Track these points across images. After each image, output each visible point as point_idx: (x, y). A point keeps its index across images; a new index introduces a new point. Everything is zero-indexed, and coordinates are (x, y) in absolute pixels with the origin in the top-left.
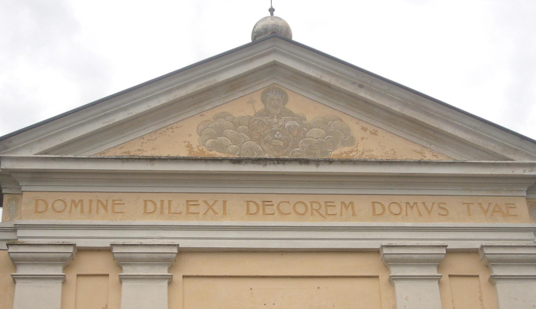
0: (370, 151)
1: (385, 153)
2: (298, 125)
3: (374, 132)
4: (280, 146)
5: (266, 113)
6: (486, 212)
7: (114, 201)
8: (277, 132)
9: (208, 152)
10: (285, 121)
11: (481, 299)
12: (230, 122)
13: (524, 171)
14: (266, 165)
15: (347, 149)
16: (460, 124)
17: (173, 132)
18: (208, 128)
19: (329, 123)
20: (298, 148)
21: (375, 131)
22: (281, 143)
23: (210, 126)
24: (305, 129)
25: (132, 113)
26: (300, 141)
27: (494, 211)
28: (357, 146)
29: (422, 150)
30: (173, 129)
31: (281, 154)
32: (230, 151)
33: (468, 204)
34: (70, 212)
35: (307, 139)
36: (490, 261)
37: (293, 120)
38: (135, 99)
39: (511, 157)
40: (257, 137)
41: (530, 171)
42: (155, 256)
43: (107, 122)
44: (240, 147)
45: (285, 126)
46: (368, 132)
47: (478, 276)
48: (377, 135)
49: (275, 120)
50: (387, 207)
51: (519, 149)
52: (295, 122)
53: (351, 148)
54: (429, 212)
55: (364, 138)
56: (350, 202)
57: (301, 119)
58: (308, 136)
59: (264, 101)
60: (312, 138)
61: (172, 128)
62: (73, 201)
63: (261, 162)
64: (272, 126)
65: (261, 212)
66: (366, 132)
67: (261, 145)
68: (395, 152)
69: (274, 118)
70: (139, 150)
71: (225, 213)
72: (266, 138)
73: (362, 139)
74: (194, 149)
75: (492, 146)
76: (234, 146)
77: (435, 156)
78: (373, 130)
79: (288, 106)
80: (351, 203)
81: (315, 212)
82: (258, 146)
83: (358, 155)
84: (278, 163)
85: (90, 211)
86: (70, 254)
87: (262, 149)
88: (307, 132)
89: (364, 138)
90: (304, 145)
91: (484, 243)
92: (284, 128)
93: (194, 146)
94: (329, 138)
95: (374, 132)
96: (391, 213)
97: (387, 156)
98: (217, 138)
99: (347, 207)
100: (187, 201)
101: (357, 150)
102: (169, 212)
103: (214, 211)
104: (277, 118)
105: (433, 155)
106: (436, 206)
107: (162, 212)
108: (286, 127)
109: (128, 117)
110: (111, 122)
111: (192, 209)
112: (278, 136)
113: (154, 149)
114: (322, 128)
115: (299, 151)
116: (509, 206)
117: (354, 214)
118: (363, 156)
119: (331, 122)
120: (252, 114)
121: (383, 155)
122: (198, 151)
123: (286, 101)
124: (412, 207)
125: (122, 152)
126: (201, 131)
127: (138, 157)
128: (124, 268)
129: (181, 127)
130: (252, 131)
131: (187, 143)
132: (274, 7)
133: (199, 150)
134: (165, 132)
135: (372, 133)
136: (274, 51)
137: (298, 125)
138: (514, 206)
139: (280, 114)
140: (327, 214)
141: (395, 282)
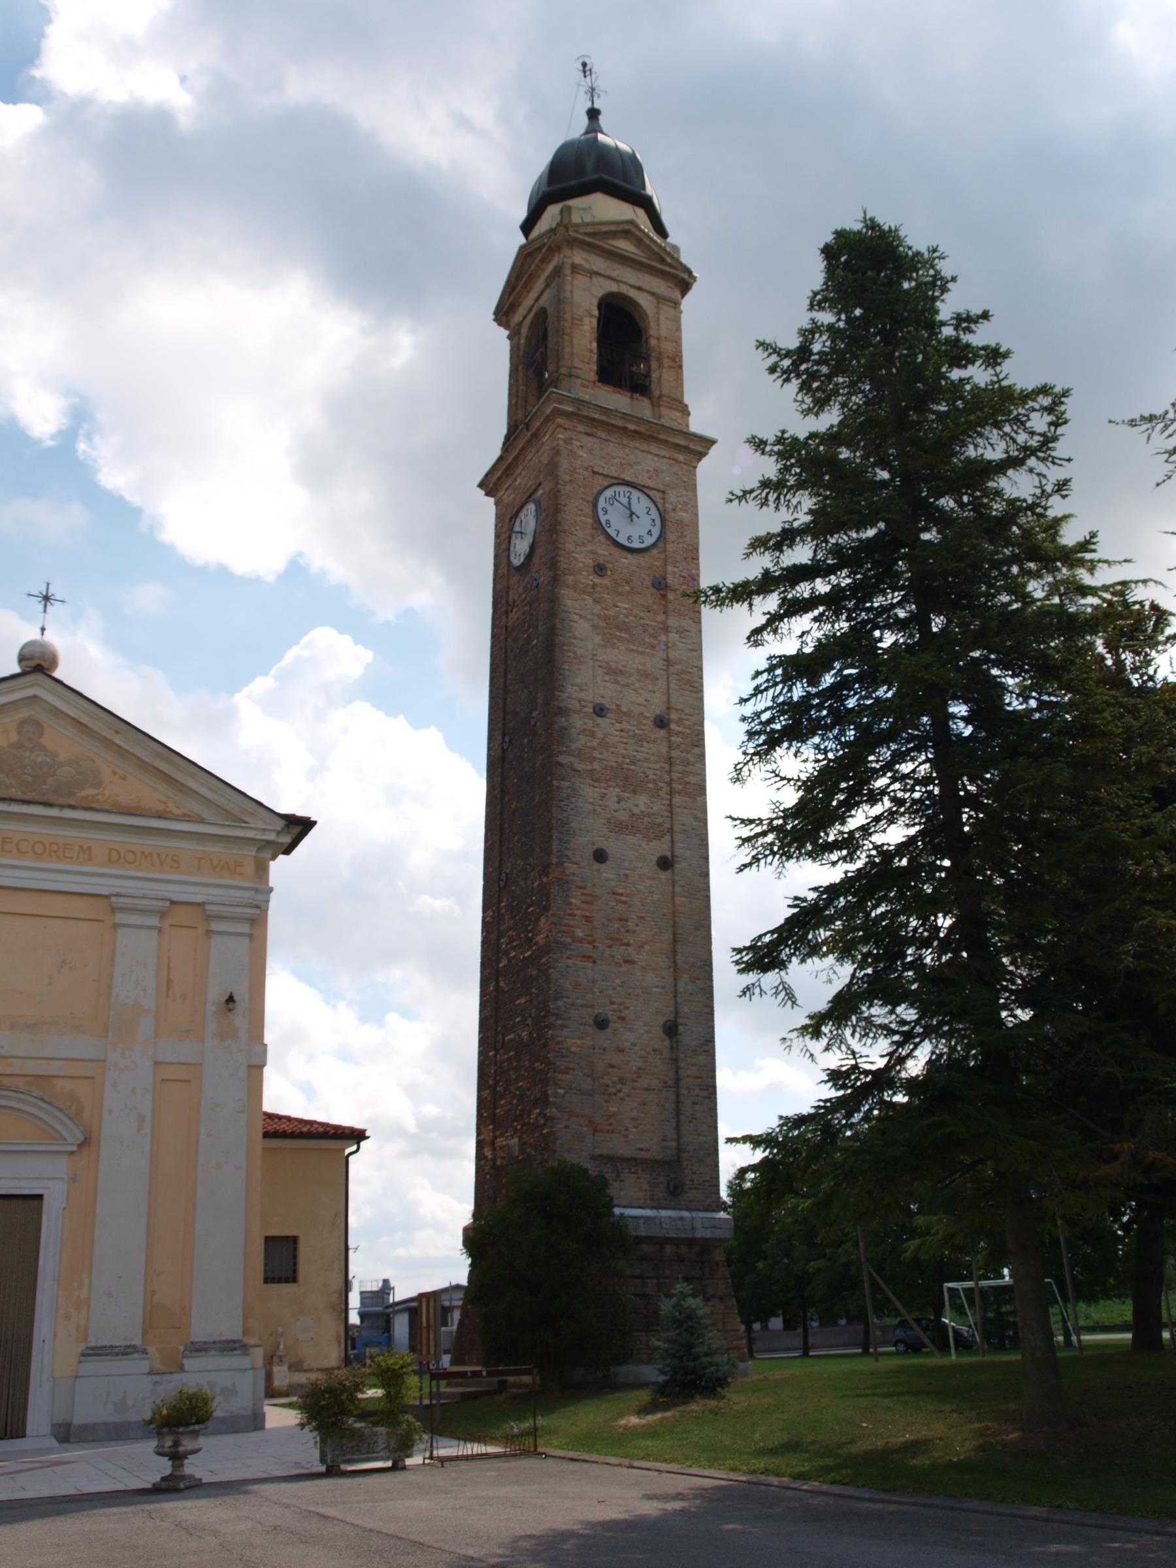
6: (214, 868)
15: (93, 791)
22: (30, 779)
33: (200, 858)
39: (246, 819)
47: (196, 928)
49: (28, 754)
54: (162, 864)
59: (19, 732)
73: (111, 782)
79: (45, 741)
80: (89, 848)
91: (210, 898)
96: (126, 861)
99: (84, 851)
123: (41, 735)
124: (146, 857)
136: (36, 684)
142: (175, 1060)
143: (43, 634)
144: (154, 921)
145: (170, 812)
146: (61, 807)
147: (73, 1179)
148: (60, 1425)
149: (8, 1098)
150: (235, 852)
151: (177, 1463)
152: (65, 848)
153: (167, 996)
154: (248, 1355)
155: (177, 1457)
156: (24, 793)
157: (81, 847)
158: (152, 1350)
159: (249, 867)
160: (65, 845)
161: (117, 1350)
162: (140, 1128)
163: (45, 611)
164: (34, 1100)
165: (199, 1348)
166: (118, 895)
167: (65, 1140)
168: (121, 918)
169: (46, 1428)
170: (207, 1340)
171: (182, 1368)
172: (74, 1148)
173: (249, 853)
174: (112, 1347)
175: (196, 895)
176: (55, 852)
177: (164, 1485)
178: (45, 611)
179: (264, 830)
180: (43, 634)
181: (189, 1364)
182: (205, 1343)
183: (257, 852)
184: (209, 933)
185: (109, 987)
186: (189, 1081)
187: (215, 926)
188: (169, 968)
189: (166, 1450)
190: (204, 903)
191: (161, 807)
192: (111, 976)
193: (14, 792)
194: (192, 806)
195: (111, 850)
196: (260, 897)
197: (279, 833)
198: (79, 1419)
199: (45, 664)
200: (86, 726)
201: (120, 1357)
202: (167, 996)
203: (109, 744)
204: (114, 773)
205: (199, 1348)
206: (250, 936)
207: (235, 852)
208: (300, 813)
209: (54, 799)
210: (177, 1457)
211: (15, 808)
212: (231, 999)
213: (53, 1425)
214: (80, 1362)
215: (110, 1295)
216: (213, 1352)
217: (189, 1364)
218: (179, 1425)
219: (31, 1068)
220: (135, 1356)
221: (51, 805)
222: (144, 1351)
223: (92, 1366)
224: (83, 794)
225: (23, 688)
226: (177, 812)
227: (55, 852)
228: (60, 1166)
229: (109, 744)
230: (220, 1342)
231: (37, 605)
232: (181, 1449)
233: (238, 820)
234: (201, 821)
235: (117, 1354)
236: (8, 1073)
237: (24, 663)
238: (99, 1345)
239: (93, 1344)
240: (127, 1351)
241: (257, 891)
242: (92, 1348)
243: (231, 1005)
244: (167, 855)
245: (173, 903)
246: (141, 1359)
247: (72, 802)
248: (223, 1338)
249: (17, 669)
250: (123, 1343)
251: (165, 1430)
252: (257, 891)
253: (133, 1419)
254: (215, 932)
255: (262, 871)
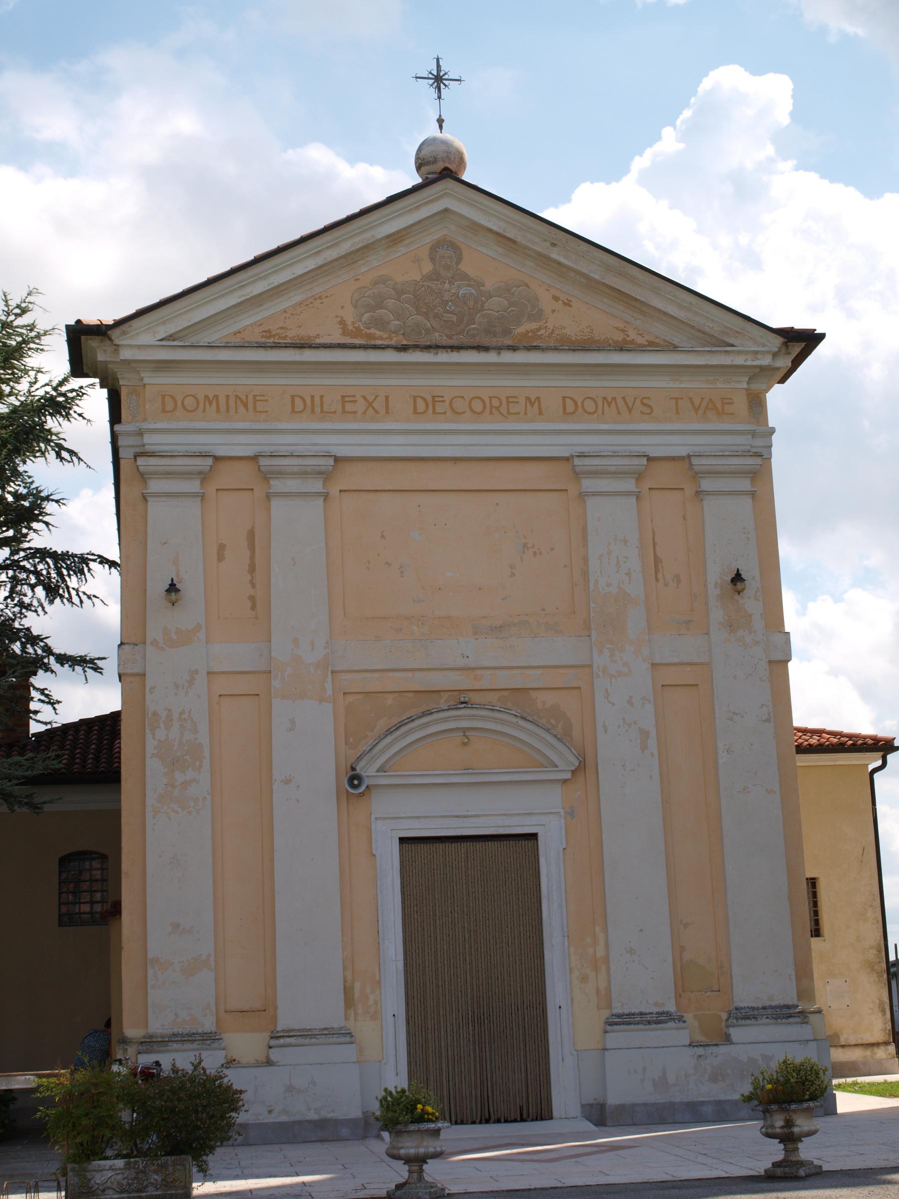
0: (561, 329)
1: (580, 331)
2: (475, 293)
3: (567, 302)
4: (453, 322)
5: (434, 276)
6: (697, 410)
7: (254, 396)
8: (450, 303)
9: (366, 330)
10: (459, 287)
11: (684, 518)
12: (391, 290)
13: (746, 360)
14: (437, 353)
15: (534, 326)
16: (672, 298)
17: (322, 303)
18: (365, 297)
19: (513, 290)
20: (474, 324)
21: (568, 301)
22: (454, 318)
23: (366, 295)
24: (483, 298)
25: (273, 283)
26: (476, 315)
27: (707, 408)
28: (546, 322)
29: (625, 327)
30: (322, 299)
31: (454, 333)
32: (393, 329)
34: (204, 411)
35: (485, 312)
36: (697, 473)
37: (469, 286)
38: (277, 265)
39: (731, 341)
40: (425, 310)
41: (752, 360)
42: (309, 469)
43: (243, 296)
44: (404, 323)
45: (458, 295)
46: (560, 302)
48: (571, 306)
49: (447, 286)
50: (580, 404)
51: (742, 331)
52: (469, 288)
53: (539, 324)
54: (630, 410)
55: (555, 310)
56: (537, 398)
57: (479, 284)
58: (488, 308)
59: (432, 259)
60: (492, 310)
61: (320, 298)
62: (206, 397)
63: (432, 350)
64: (442, 294)
65: (430, 410)
66: (557, 301)
67: (429, 321)
68: (592, 330)
69: (445, 283)
70: (282, 328)
71: (387, 412)
72: (436, 311)
73: (553, 311)
74: (349, 327)
75: (709, 327)
76: (397, 322)
77: (640, 335)
78: (567, 299)
79: (464, 267)
80: (538, 399)
81: (494, 411)
82: (426, 322)
83: (547, 333)
84: (452, 351)
85: (228, 411)
86: (209, 467)
87: (431, 327)
88: (485, 303)
89: (555, 310)
90: (482, 320)
92: (458, 297)
93: (349, 322)
94: (513, 311)
95: (567, 302)
97: (583, 336)
98: (377, 312)
100: (343, 397)
101: (546, 327)
102: (322, 411)
103: (373, 408)
104: (449, 283)
105: (638, 334)
106: (638, 402)
107: (313, 411)
108: (460, 295)
109: (269, 288)
110: (248, 295)
111: (349, 407)
112: (450, 308)
113: (300, 327)
114: (503, 298)
115: (475, 329)
116: (725, 401)
117: (541, 413)
118: (553, 336)
119: (515, 288)
120: (418, 278)
121: (578, 334)
122: (354, 330)
124: (609, 404)
125: (261, 331)
126: (357, 302)
127: (284, 345)
128: (272, 482)
129: (331, 296)
130: (418, 301)
131: (339, 319)
132: (443, 117)
133: (354, 327)
134: (311, 303)
135: (565, 304)
136: (447, 194)
137: (475, 293)
138: (731, 401)
139: (452, 278)
140: (509, 413)
141: (586, 498)
142: (676, 660)
143: (441, 127)
144: (629, 485)
145: (632, 342)
146: (499, 349)
147: (571, 813)
148: (591, 1105)
149: (483, 718)
150: (720, 385)
151: (790, 1146)
152: (508, 402)
153: (657, 580)
154: (807, 1023)
155: (789, 1139)
156: (450, 337)
157: (528, 399)
158: (688, 1017)
159: (741, 404)
160: (507, 398)
161: (648, 1018)
162: (644, 747)
163: (439, 97)
164: (514, 720)
165: (747, 1015)
166: (582, 456)
167: (557, 767)
168: (588, 484)
169: (575, 1111)
170: (754, 1005)
171: (727, 1039)
172: (568, 776)
173: (740, 386)
174: (641, 1014)
175: (678, 446)
176: (497, 408)
177: (779, 1171)
178: (439, 97)
179: (757, 352)
180: (441, 127)
181: (736, 1033)
182: (753, 1008)
183: (748, 383)
184: (699, 494)
185: (585, 574)
186: (697, 685)
187: (706, 484)
188: (655, 544)
189: (778, 1130)
190: (689, 456)
191: (619, 337)
192: (585, 559)
193: (437, 337)
194: (659, 330)
195: (564, 398)
196: (758, 442)
197: (775, 355)
198: (613, 1099)
199: (452, 167)
200: (514, 242)
201: (654, 1026)
202: (657, 580)
203: (544, 260)
204: (556, 299)
205: (747, 1015)
206: (753, 494)
207: (720, 385)
208: (800, 324)
209: (486, 341)
210: (789, 1139)
211: (444, 357)
212: (737, 578)
213: (583, 1106)
214: (606, 1032)
215: (631, 952)
216: (765, 1020)
217: (736, 1033)
218: (791, 1101)
219: (503, 680)
220: (671, 1024)
221: (486, 349)
222: (681, 1019)
223: (619, 1037)
224: (521, 330)
225: (431, 201)
226: (640, 340)
227: (497, 408)
228: (553, 798)
229: (544, 260)
230: (771, 1007)
231: (426, 89)
232: (796, 1130)
233: (721, 344)
234: (674, 348)
235: (649, 1023)
236: (477, 688)
237: (424, 169)
238: (626, 1012)
239: (618, 1010)
240: (661, 1018)
241: (754, 434)
242: (619, 1016)
243: (739, 586)
244: (635, 398)
245: (650, 459)
246: (678, 1029)
247: (508, 342)
248: (774, 1003)
249: (418, 180)
250: (655, 1010)
251: (774, 1107)
252: (754, 434)
253: (677, 1100)
254: (708, 493)
255: (757, 405)
